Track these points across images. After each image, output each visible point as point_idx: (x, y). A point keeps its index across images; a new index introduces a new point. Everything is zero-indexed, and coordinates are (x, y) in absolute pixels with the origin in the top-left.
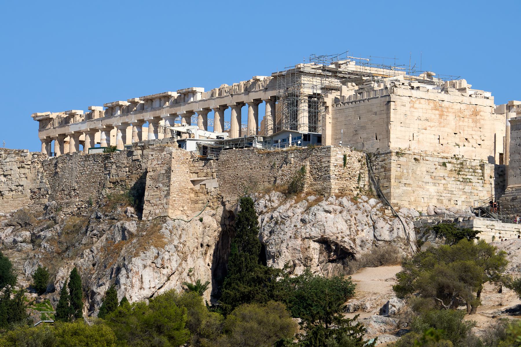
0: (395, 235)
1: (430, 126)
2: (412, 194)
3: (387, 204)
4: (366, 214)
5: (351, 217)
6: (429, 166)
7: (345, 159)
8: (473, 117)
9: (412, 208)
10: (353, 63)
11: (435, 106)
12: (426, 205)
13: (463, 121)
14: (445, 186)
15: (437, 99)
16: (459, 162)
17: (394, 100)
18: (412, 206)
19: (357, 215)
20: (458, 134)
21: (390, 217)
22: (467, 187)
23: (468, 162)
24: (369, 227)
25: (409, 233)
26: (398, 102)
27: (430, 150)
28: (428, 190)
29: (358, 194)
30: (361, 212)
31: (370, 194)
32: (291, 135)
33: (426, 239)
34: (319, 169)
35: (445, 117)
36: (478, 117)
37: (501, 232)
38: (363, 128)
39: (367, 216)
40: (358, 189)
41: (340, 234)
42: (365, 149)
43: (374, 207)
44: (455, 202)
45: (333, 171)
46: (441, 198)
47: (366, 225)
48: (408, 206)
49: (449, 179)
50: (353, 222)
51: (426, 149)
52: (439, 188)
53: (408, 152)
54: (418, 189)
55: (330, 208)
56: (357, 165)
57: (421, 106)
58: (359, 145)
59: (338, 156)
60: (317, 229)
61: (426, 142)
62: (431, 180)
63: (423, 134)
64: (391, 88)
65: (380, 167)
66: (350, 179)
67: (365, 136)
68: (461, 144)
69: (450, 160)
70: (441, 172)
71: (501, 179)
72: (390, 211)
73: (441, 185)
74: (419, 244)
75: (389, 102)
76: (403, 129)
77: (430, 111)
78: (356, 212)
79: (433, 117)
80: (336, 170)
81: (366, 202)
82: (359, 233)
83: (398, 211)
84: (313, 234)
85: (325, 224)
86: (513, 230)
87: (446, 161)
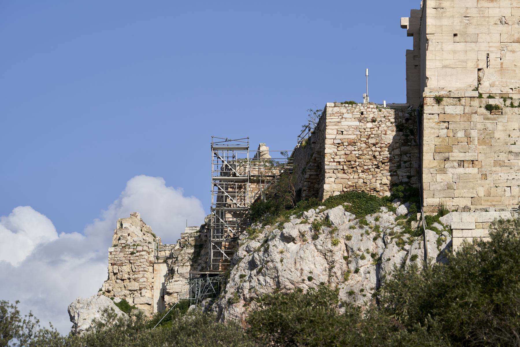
19: (348, 238)
47: (363, 258)
54: (498, 169)
59: (345, 124)
63: (513, 52)
76: (460, 46)
80: (343, 152)
84: (262, 291)
85: (279, 265)
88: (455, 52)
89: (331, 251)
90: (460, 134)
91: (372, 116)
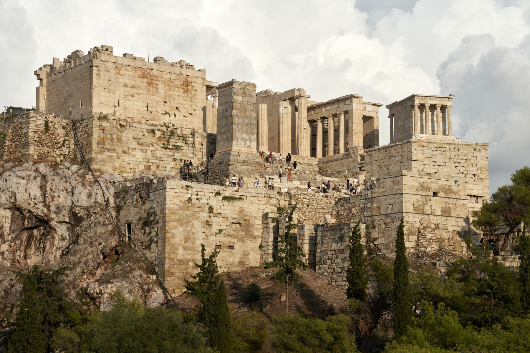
0: (93, 200)
1: (137, 93)
3: (90, 169)
4: (64, 180)
9: (116, 174)
11: (143, 74)
13: (173, 91)
17: (97, 65)
19: (54, 180)
20: (168, 103)
21: (90, 182)
24: (68, 192)
25: (108, 199)
26: (102, 68)
27: (137, 117)
29: (61, 161)
30: (60, 177)
31: (73, 161)
33: (125, 203)
34: (20, 136)
37: (199, 193)
38: (70, 96)
40: (62, 156)
41: (33, 200)
42: (72, 117)
43: (76, 173)
44: (164, 168)
47: (63, 191)
48: (112, 172)
53: (113, 118)
54: (124, 154)
55: (24, 174)
56: (61, 132)
57: (127, 72)
58: (67, 114)
62: (138, 147)
63: (129, 100)
65: (83, 133)
66: (53, 145)
67: (72, 104)
68: (171, 112)
69: (159, 127)
70: (149, 139)
71: (212, 147)
72: (91, 177)
74: (118, 209)
75: (92, 66)
76: (107, 94)
77: (137, 79)
78: (53, 177)
79: (141, 84)
81: (69, 169)
82: (55, 199)
86: (213, 191)
87: (154, 128)
88: (105, 97)
90: (109, 136)
91: (51, 120)
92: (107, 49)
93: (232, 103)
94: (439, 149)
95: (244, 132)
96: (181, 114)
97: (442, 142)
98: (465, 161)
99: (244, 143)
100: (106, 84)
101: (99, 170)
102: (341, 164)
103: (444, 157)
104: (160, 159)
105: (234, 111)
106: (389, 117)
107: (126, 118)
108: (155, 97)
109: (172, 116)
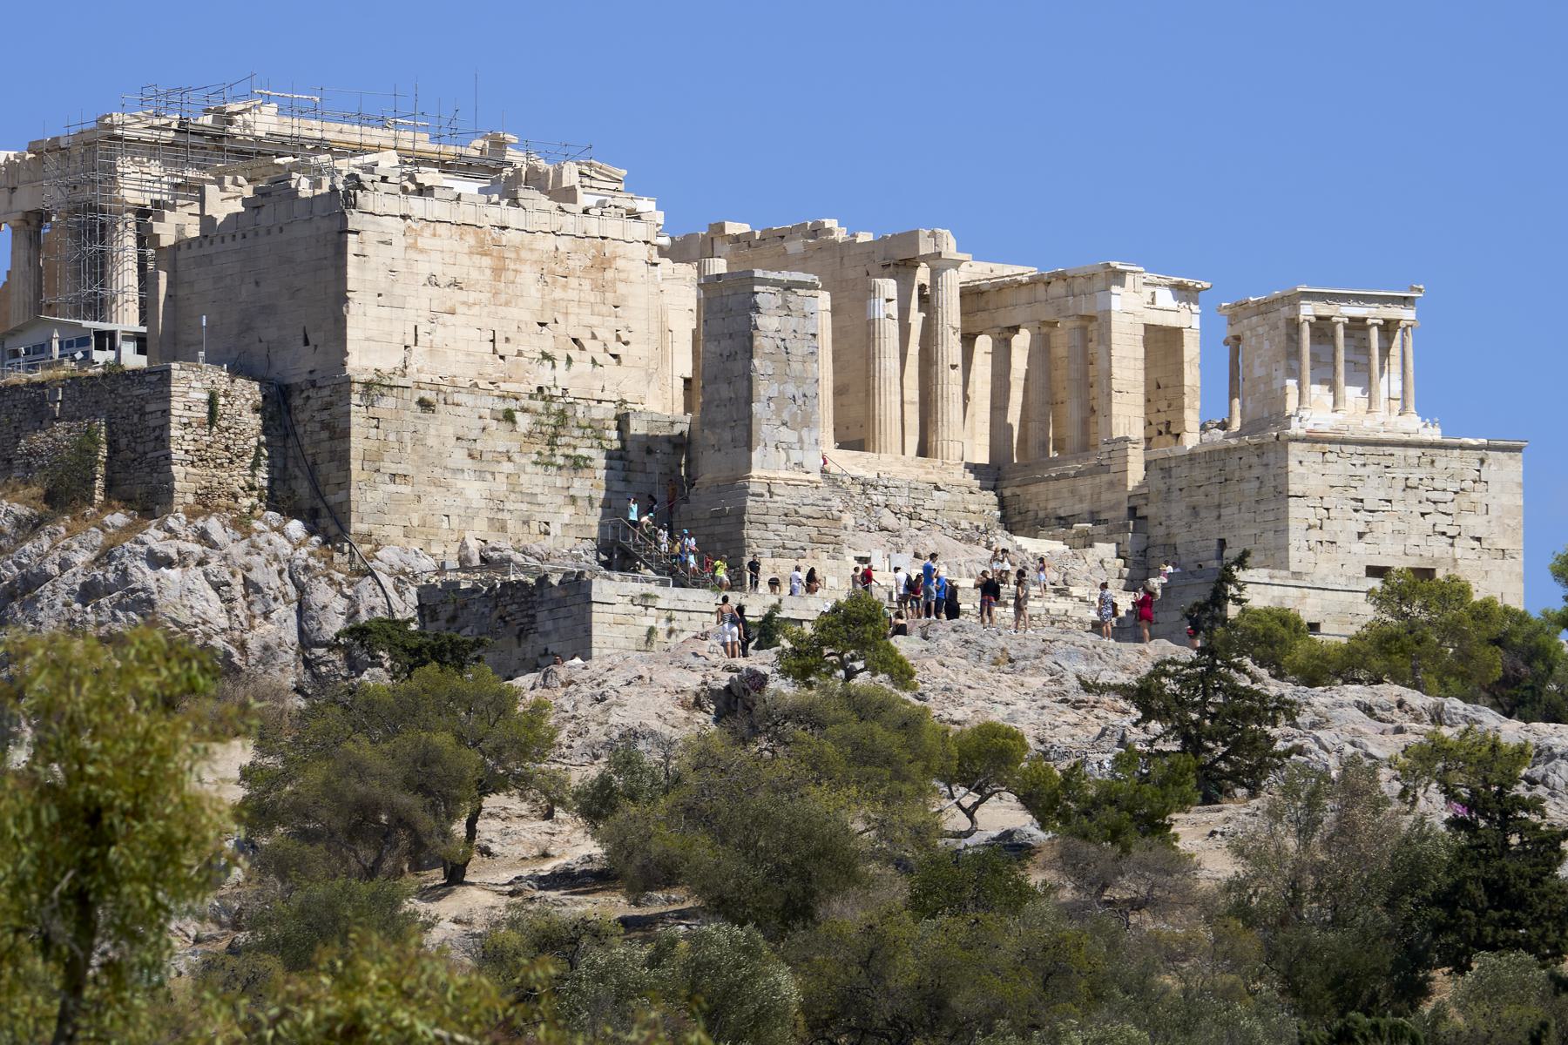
1: (464, 303)
2: (415, 506)
4: (276, 566)
5: (233, 575)
6: (464, 421)
7: (212, 402)
8: (595, 274)
10: (272, 109)
11: (482, 243)
12: (455, 537)
13: (565, 287)
14: (513, 480)
15: (486, 223)
16: (554, 407)
17: (357, 227)
18: (413, 541)
20: (551, 325)
22: (577, 483)
23: (580, 409)
26: (370, 235)
28: (460, 493)
29: (253, 507)
32: (56, 335)
35: (511, 275)
36: (609, 274)
39: (280, 573)
45: (181, 441)
46: (500, 516)
47: (275, 599)
49: (524, 461)
50: (238, 589)
51: (454, 370)
52: (494, 486)
53: (402, 382)
54: (433, 489)
57: (436, 243)
59: (194, 395)
60: (132, 614)
61: (458, 350)
63: (444, 325)
64: (347, 194)
69: (525, 402)
70: (500, 439)
73: (501, 478)
76: (385, 312)
77: (465, 260)
79: (475, 274)
83: (371, 556)
85: (155, 597)
87: (512, 405)
88: (379, 319)
89: (229, 585)
90: (392, 437)
92: (384, 179)
93: (751, 338)
94: (1376, 459)
95: (784, 424)
96: (587, 357)
97: (1383, 436)
98: (1450, 496)
99: (783, 453)
100: (383, 285)
101: (367, 537)
102: (1073, 492)
103: (1387, 483)
104: (531, 499)
105: (756, 362)
106: (1226, 343)
107: (437, 380)
108: (515, 313)
109: (561, 364)
